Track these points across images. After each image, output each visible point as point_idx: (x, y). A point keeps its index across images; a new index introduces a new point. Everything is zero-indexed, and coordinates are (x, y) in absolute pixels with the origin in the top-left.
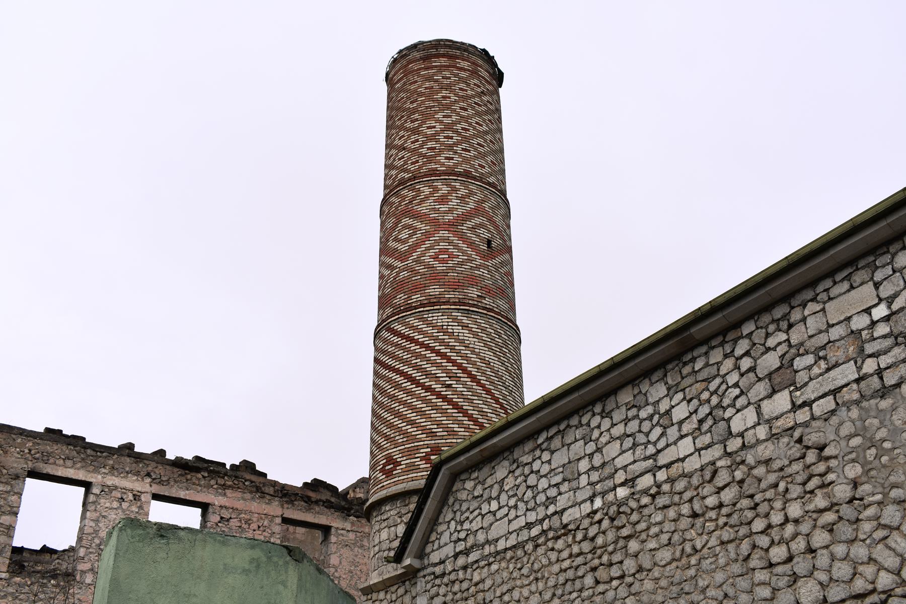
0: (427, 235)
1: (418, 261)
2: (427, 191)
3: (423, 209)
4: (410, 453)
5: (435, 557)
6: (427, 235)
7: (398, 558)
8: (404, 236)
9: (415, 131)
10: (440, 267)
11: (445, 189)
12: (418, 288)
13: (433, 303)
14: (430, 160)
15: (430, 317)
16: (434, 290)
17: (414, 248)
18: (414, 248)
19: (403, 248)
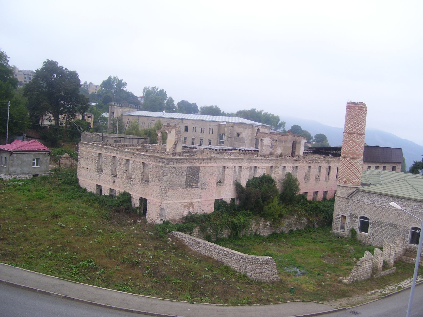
0: (355, 146)
1: (353, 150)
2: (356, 137)
3: (355, 140)
4: (349, 181)
5: (354, 199)
6: (355, 146)
7: (348, 197)
8: (351, 144)
9: (355, 123)
10: (356, 152)
11: (359, 137)
12: (352, 155)
13: (355, 158)
14: (357, 130)
15: (354, 161)
16: (355, 156)
17: (353, 147)
18: (353, 147)
19: (351, 146)
